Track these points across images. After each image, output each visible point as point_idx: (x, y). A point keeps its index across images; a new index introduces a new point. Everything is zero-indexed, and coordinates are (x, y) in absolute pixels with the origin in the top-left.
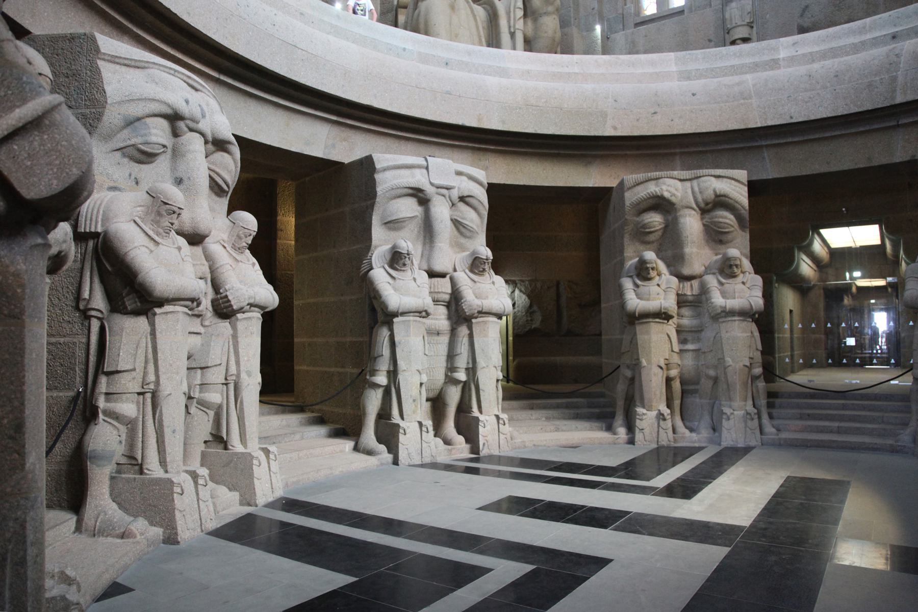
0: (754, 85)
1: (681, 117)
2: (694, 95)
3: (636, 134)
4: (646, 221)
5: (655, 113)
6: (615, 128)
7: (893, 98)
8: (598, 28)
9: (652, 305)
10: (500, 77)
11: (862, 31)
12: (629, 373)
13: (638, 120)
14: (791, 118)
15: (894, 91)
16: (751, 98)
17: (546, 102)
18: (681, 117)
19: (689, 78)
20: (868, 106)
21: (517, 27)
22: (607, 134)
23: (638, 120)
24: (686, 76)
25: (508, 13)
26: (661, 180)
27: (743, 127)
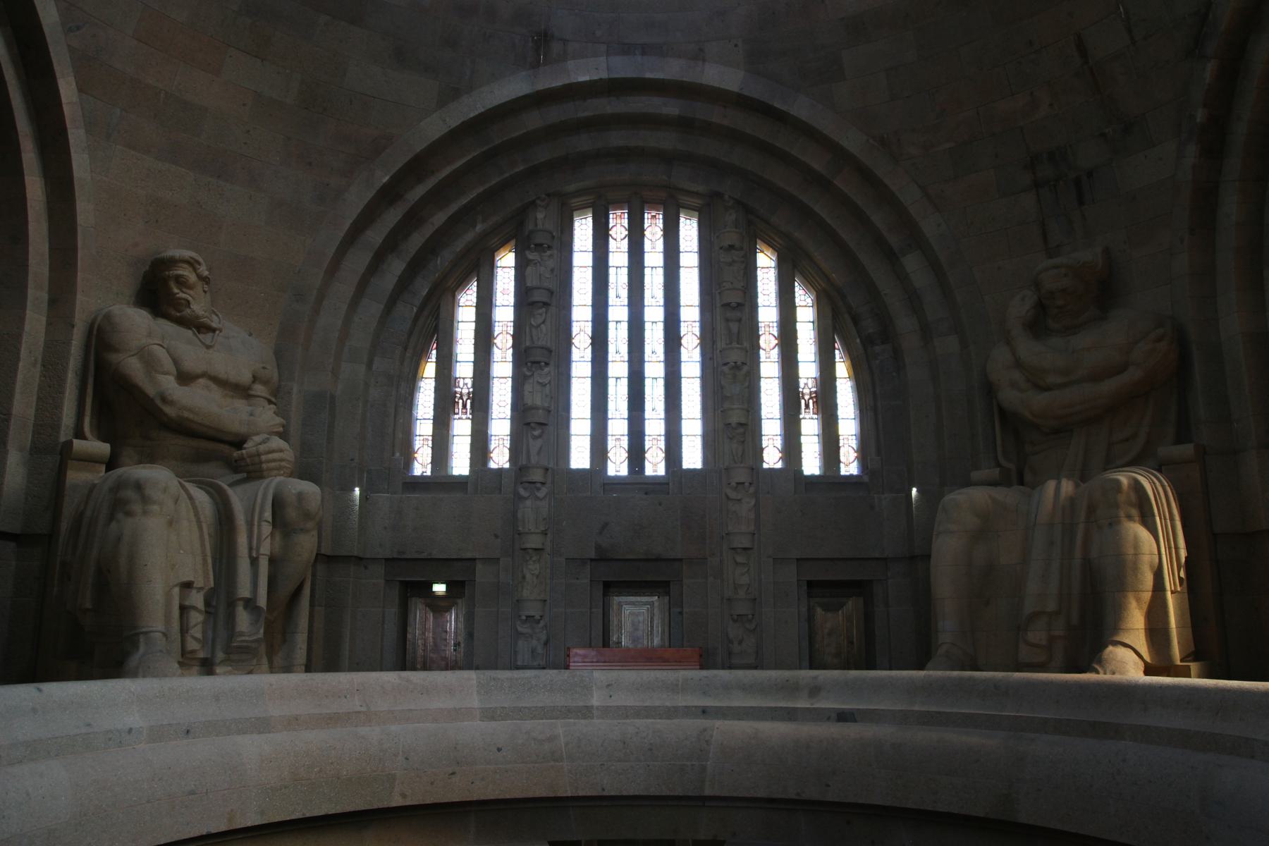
0: (567, 744)
1: (483, 779)
2: (499, 750)
3: (428, 802)
5: (453, 773)
6: (404, 796)
8: (357, 491)
10: (260, 733)
11: (674, 688)
17: (320, 771)
18: (483, 779)
19: (493, 718)
20: (679, 792)
21: (262, 551)
22: (394, 804)
24: (490, 715)
25: (250, 524)
27: (551, 795)
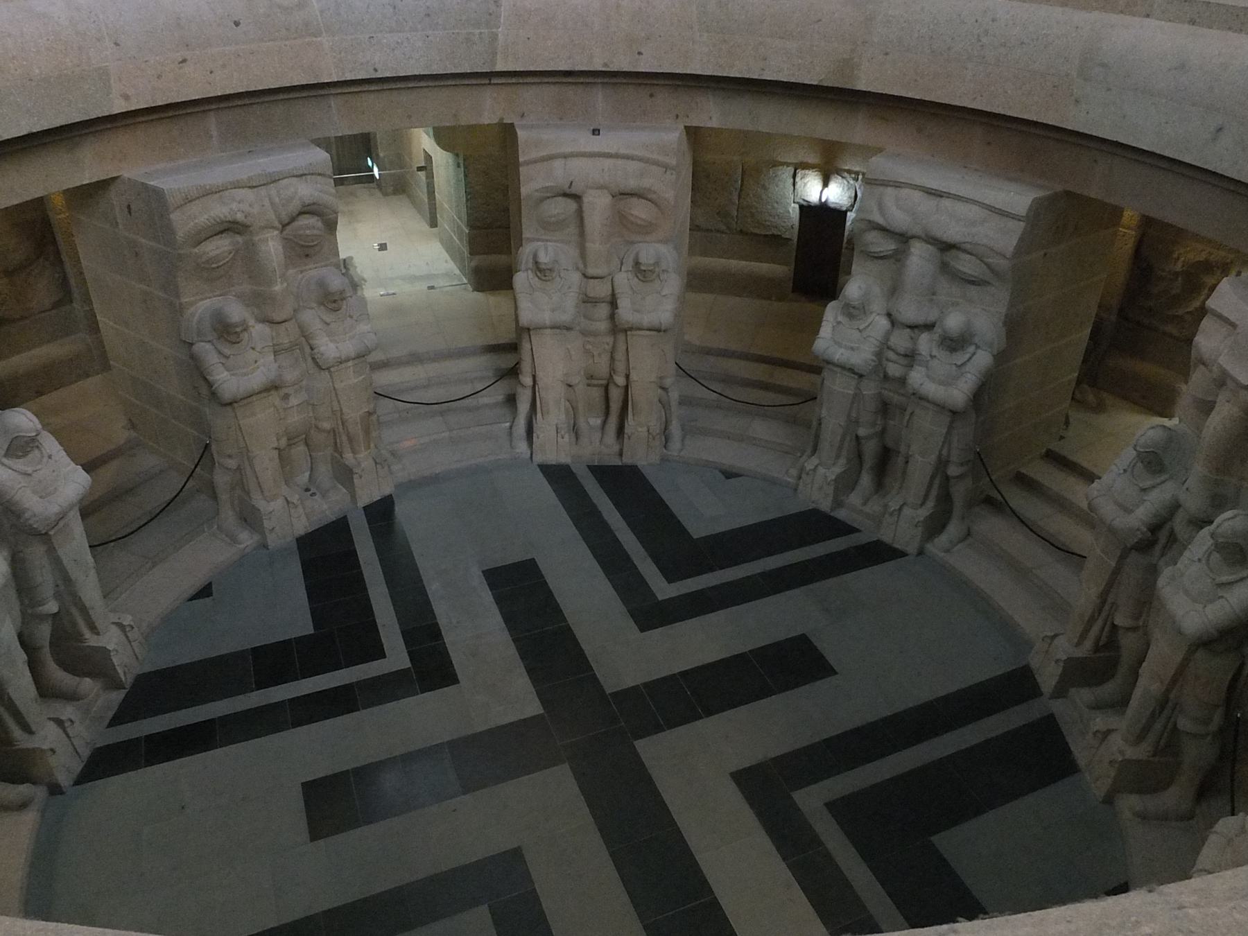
1: (224, 66)
2: (237, 24)
4: (211, 254)
5: (184, 61)
6: (126, 98)
7: (494, 63)
9: (257, 379)
12: (232, 463)
13: (159, 77)
14: (376, 70)
15: (495, 54)
16: (320, 34)
23: (159, 77)
26: (227, 193)
